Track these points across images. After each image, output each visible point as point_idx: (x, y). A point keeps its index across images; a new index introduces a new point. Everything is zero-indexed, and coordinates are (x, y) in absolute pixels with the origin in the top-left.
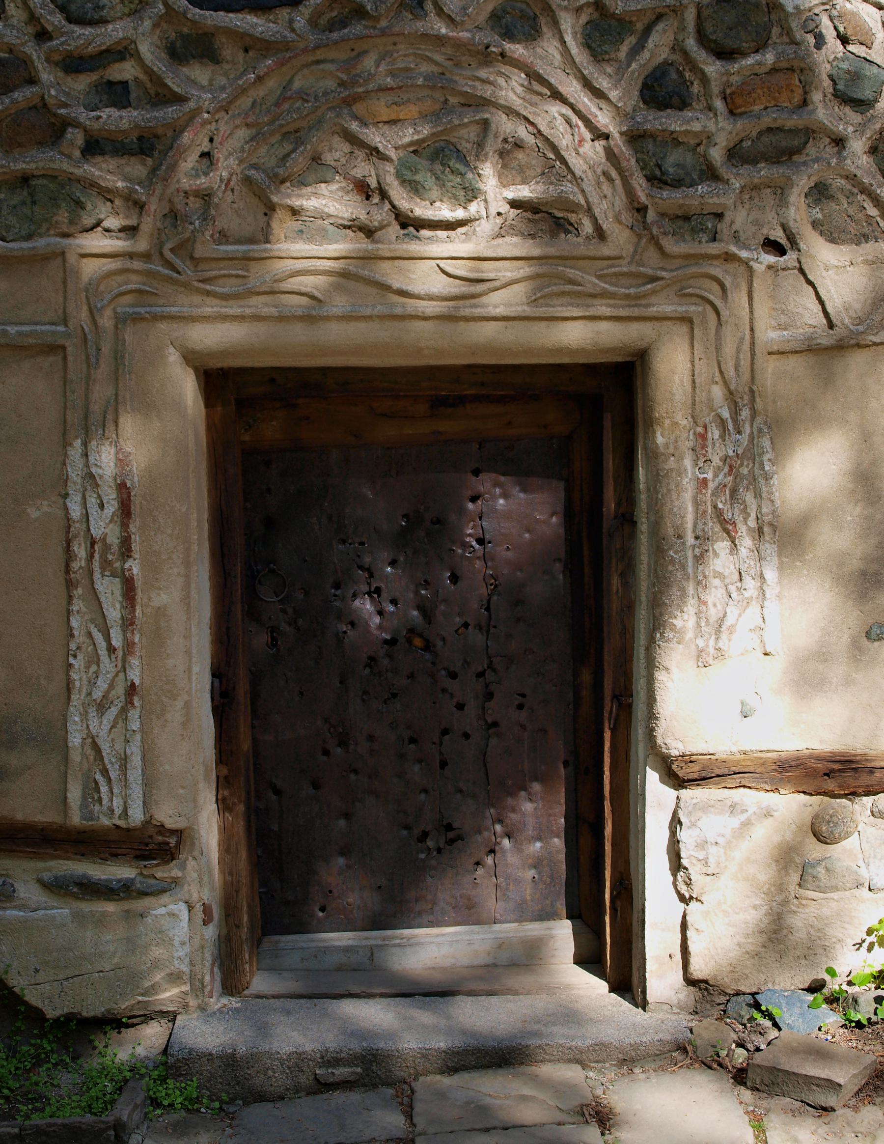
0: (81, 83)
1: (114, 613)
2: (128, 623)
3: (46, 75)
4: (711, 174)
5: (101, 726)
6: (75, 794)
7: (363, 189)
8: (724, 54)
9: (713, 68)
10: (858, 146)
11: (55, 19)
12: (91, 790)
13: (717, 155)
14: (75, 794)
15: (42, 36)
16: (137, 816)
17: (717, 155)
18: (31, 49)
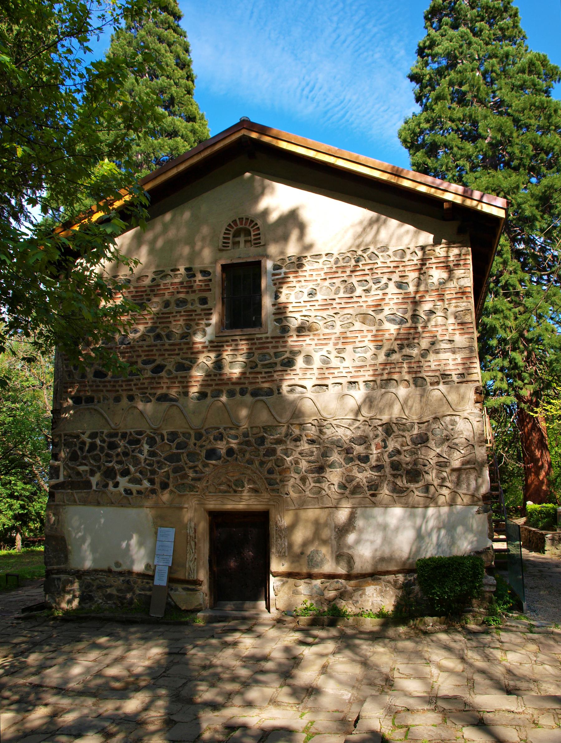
0: (191, 471)
1: (193, 547)
2: (195, 549)
3: (187, 469)
4: (277, 484)
5: (191, 564)
6: (187, 574)
7: (228, 485)
8: (278, 466)
9: (277, 468)
10: (298, 479)
11: (188, 462)
12: (189, 574)
13: (278, 481)
14: (187, 574)
15: (186, 464)
16: (195, 578)
17: (278, 481)
18: (185, 466)
